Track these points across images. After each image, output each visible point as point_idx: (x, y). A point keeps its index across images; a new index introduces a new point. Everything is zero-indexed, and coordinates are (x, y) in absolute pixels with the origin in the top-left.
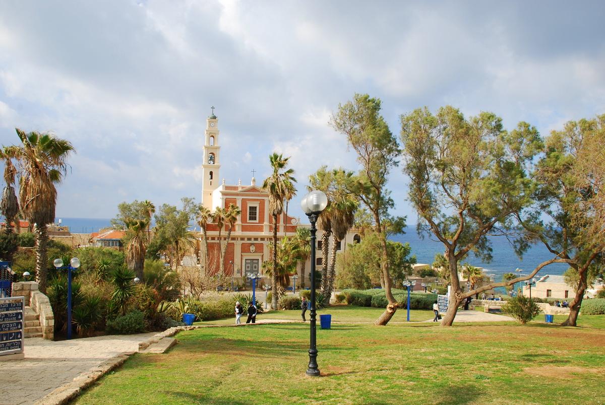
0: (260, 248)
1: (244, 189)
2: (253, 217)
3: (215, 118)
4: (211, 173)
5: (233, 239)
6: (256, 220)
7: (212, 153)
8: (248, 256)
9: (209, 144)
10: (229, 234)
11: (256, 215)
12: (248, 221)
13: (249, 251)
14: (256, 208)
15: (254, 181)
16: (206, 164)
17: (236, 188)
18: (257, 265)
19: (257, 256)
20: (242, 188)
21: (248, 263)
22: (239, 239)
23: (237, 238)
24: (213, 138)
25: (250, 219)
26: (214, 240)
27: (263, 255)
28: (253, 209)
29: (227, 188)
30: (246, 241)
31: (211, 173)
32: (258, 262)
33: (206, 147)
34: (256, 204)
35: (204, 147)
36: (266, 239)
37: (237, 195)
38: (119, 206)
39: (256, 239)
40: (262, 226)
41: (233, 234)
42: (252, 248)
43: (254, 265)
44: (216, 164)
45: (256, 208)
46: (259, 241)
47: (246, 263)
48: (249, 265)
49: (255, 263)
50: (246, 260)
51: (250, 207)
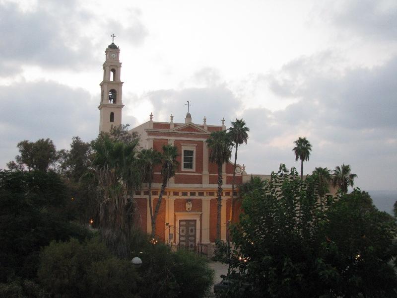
0: (198, 205)
1: (177, 128)
2: (189, 165)
6: (191, 167)
12: (183, 169)
13: (184, 209)
14: (192, 152)
20: (176, 125)
21: (183, 225)
22: (172, 193)
23: (169, 192)
26: (140, 194)
27: (201, 215)
28: (188, 153)
30: (180, 197)
31: (112, 115)
32: (196, 223)
34: (192, 148)
36: (205, 194)
37: (170, 134)
38: (19, 145)
39: (193, 194)
40: (201, 177)
42: (189, 206)
46: (197, 197)
47: (180, 225)
48: (184, 228)
49: (192, 226)
51: (185, 151)
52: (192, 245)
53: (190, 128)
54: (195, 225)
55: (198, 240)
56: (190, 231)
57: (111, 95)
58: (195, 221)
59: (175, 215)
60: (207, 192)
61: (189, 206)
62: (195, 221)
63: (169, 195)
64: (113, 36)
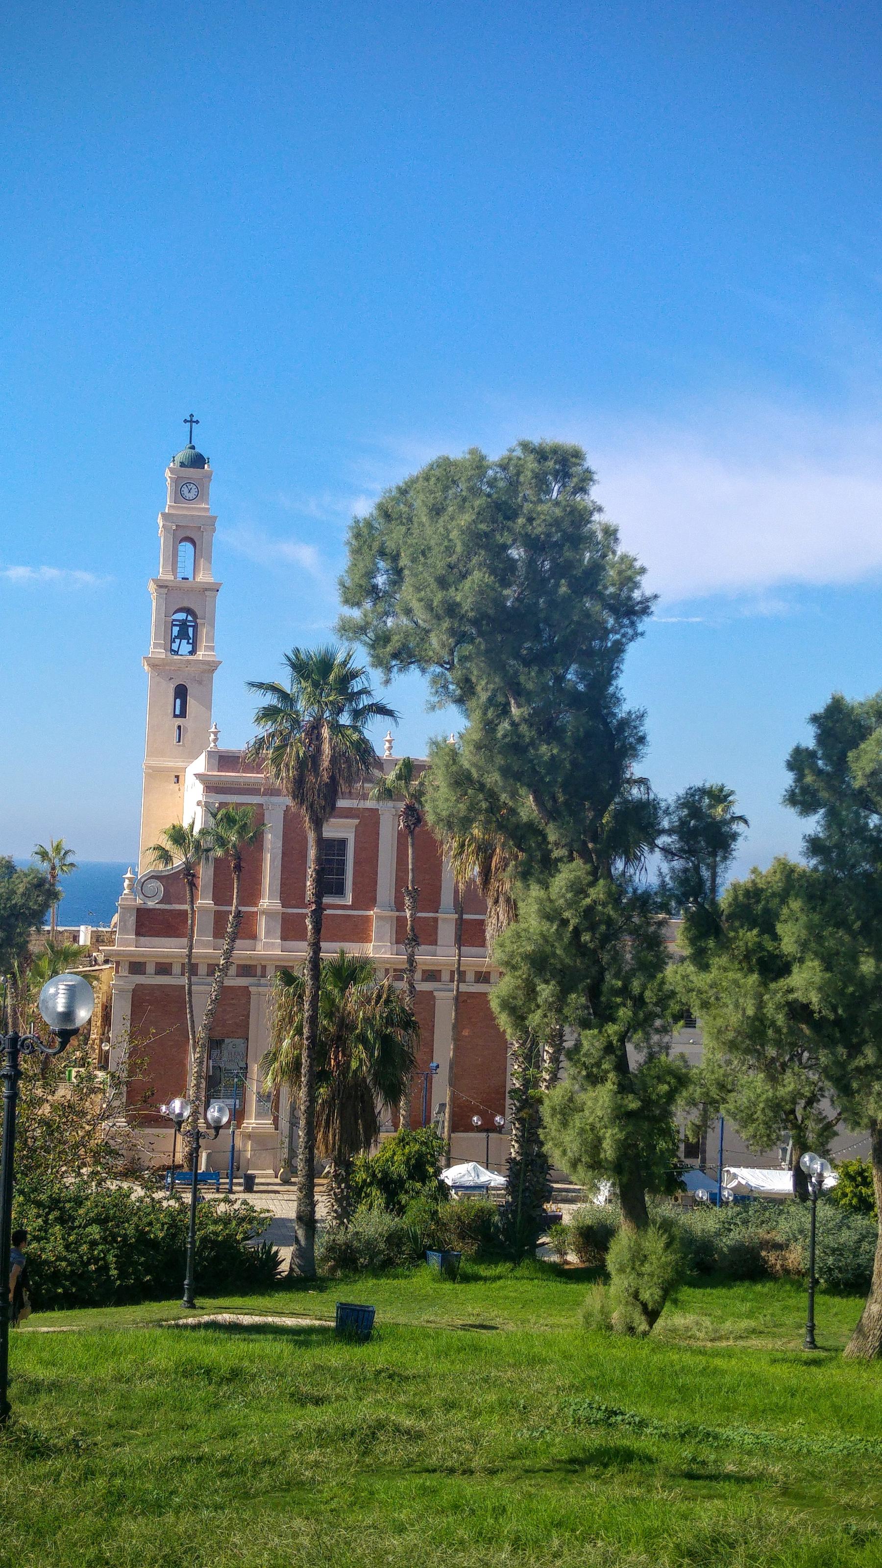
3: (198, 461)
4: (181, 692)
5: (246, 970)
7: (189, 611)
9: (174, 571)
10: (228, 954)
11: (342, 871)
14: (343, 842)
16: (161, 654)
23: (264, 968)
24: (189, 546)
33: (161, 585)
35: (152, 587)
41: (243, 952)
44: (201, 654)
45: (343, 842)
63: (264, 975)
64: (191, 421)
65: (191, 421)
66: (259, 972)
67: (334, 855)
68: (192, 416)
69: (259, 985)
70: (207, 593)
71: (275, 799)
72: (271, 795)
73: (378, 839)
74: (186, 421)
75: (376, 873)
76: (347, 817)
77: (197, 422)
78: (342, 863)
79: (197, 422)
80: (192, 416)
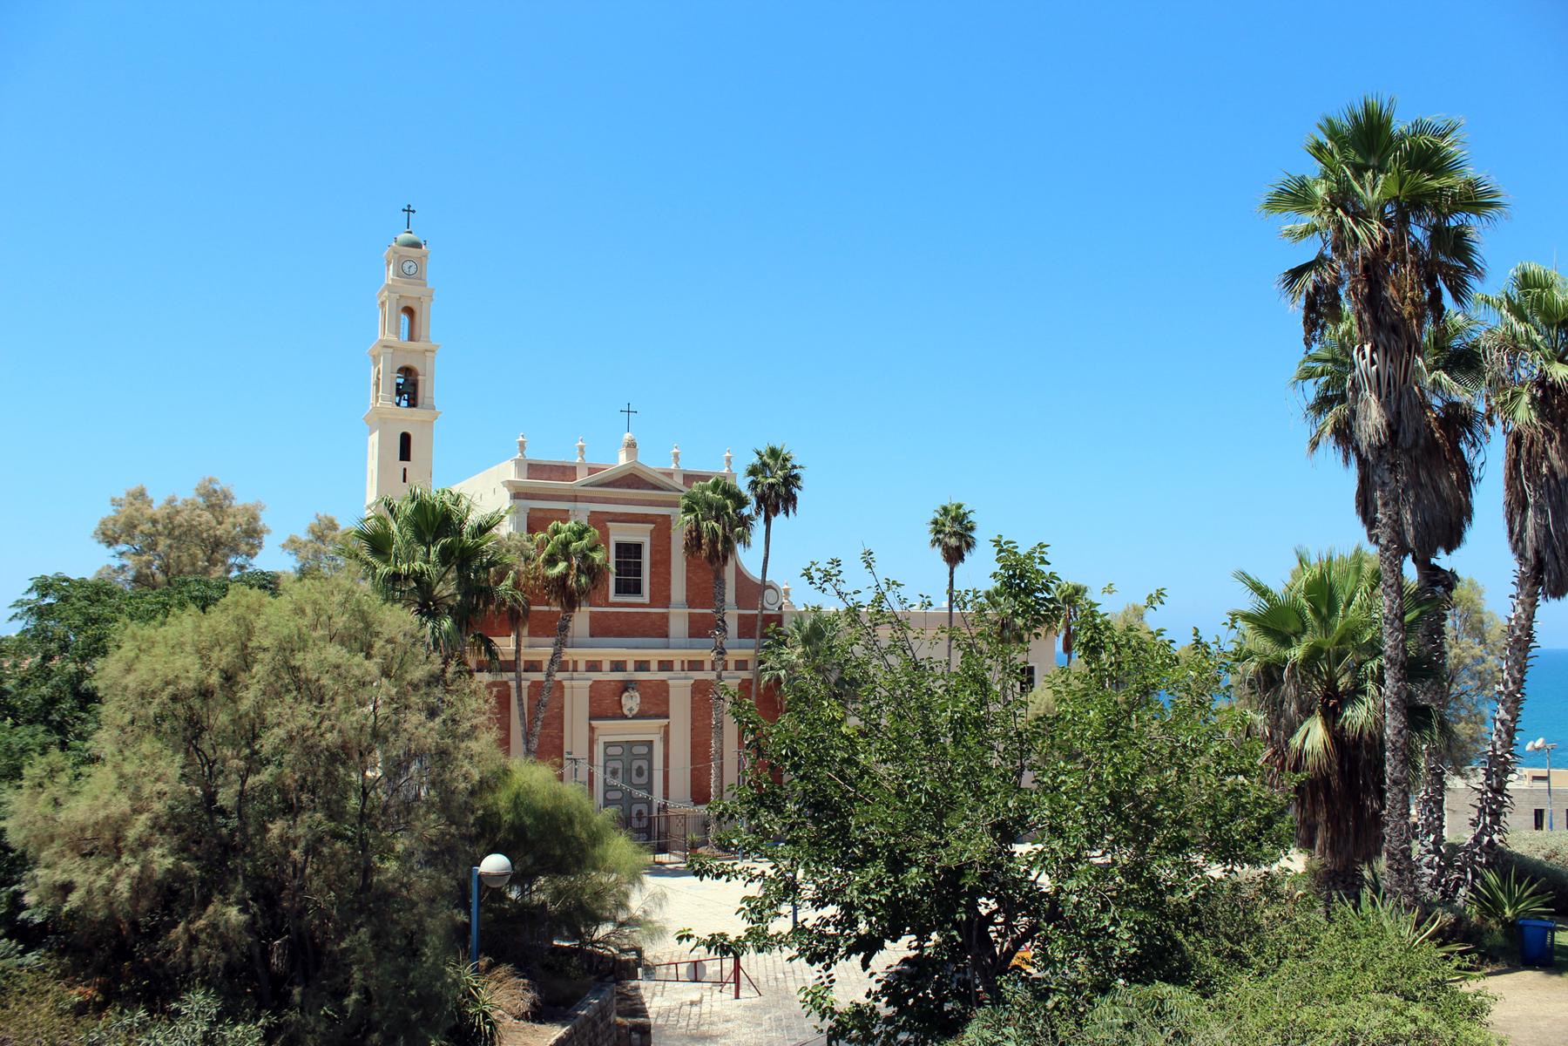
0: (656, 703)
2: (629, 585)
6: (637, 590)
8: (611, 730)
11: (639, 573)
12: (612, 597)
14: (638, 548)
15: (632, 445)
17: (566, 471)
18: (645, 765)
19: (648, 729)
20: (592, 470)
22: (582, 666)
23: (575, 662)
25: (618, 591)
27: (667, 727)
28: (629, 552)
29: (535, 469)
30: (607, 676)
31: (405, 439)
37: (575, 499)
39: (642, 666)
40: (665, 617)
42: (631, 702)
43: (636, 764)
45: (638, 548)
46: (654, 675)
50: (607, 745)
51: (619, 546)
52: (640, 813)
53: (632, 480)
54: (649, 757)
55: (658, 798)
56: (634, 772)
57: (401, 381)
58: (650, 744)
59: (592, 729)
60: (683, 662)
61: (631, 702)
62: (650, 744)
63: (575, 670)
64: (409, 210)
65: (409, 211)
66: (571, 668)
67: (631, 558)
68: (409, 206)
69: (572, 679)
70: (427, 354)
71: (580, 505)
72: (576, 501)
73: (670, 543)
74: (404, 210)
75: (669, 574)
76: (643, 522)
77: (414, 212)
78: (639, 565)
79: (414, 212)
80: (409, 206)
